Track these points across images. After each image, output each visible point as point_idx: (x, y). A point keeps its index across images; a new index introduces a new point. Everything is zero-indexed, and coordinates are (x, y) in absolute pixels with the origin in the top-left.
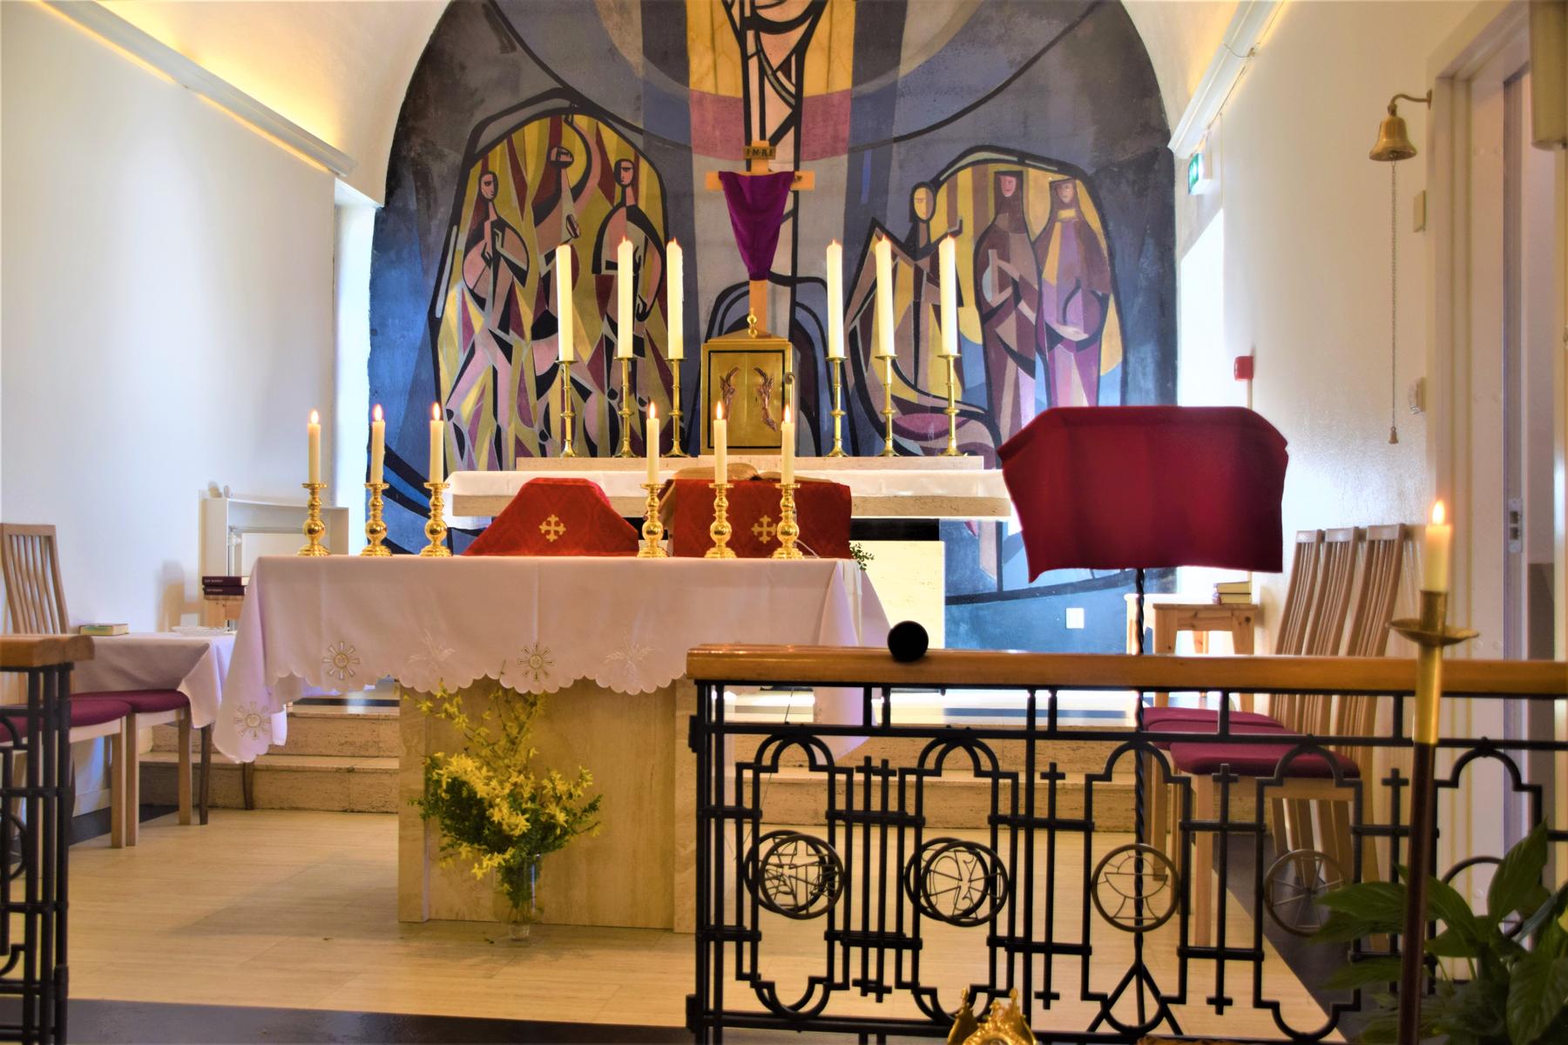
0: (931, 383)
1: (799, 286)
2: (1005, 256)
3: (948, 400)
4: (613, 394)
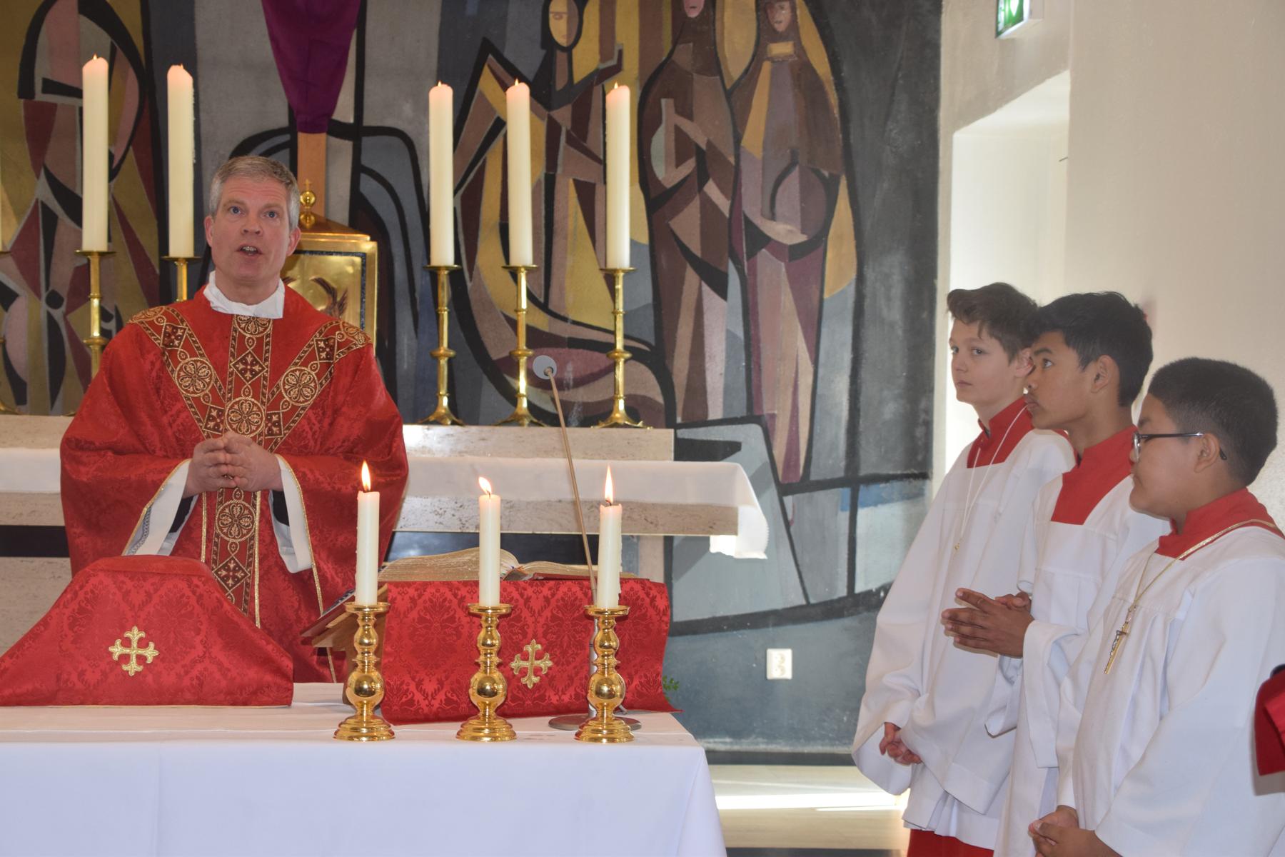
0: (570, 298)
1: (367, 141)
2: (685, 111)
3: (613, 333)
4: (54, 300)
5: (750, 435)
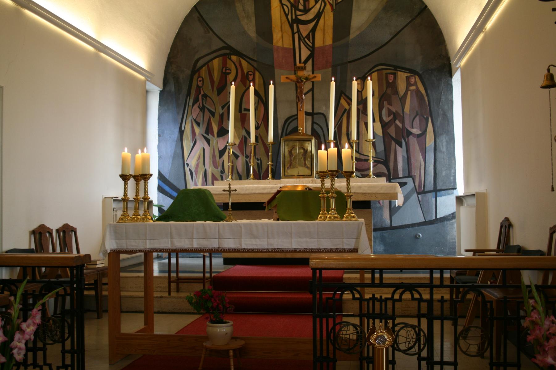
1: (315, 116)
2: (390, 104)
4: (247, 157)
5: (409, 181)
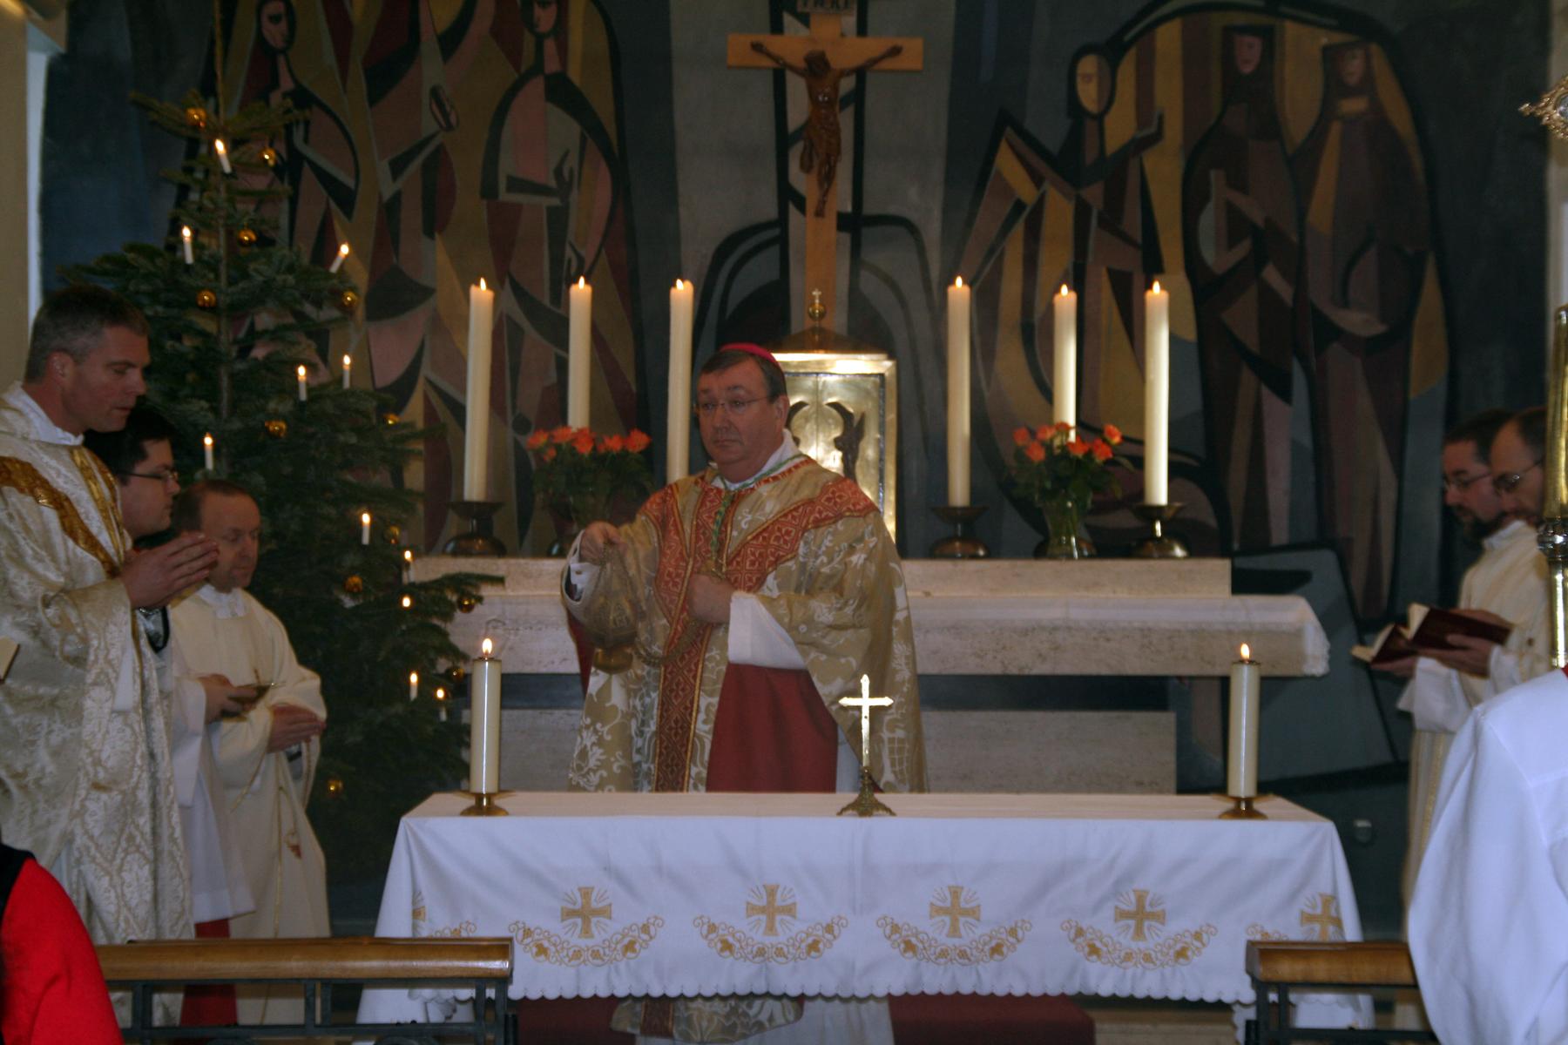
1: (867, 232)
2: (1238, 182)
5: (1323, 563)
